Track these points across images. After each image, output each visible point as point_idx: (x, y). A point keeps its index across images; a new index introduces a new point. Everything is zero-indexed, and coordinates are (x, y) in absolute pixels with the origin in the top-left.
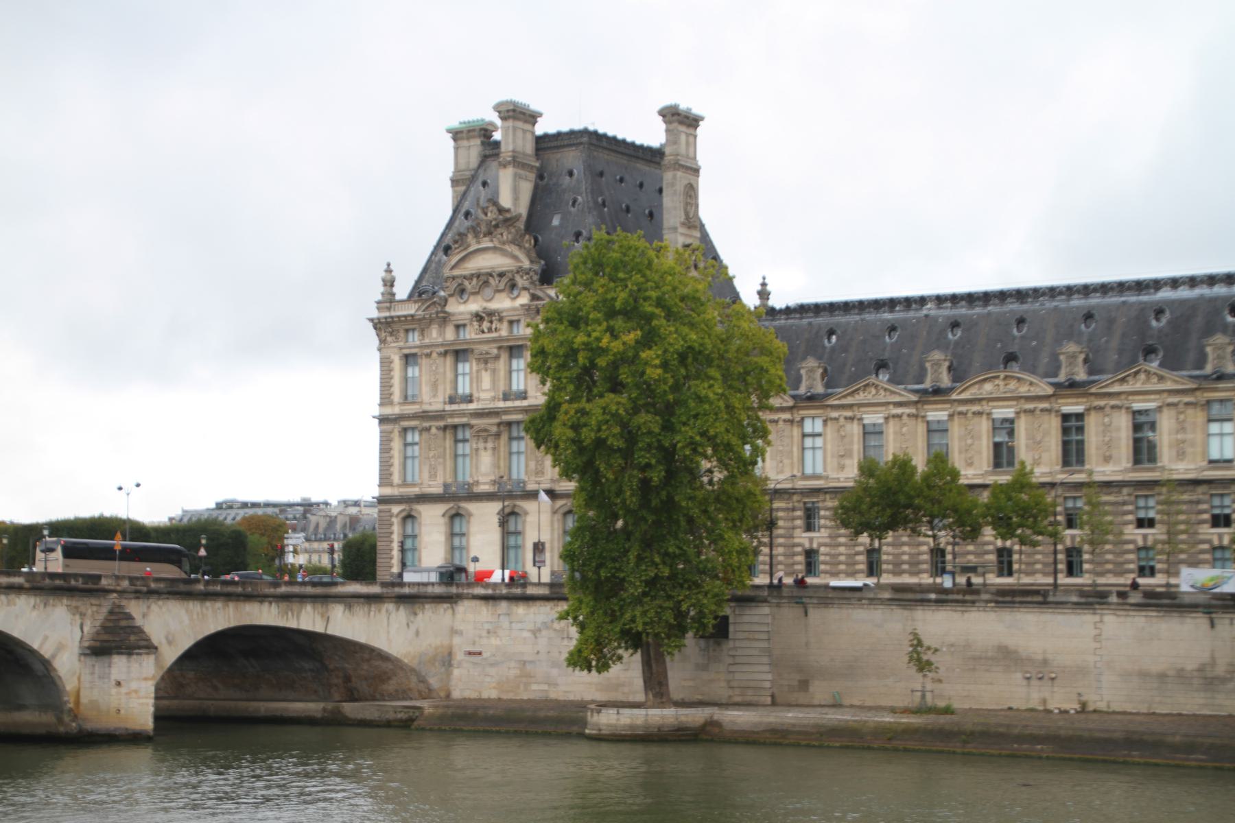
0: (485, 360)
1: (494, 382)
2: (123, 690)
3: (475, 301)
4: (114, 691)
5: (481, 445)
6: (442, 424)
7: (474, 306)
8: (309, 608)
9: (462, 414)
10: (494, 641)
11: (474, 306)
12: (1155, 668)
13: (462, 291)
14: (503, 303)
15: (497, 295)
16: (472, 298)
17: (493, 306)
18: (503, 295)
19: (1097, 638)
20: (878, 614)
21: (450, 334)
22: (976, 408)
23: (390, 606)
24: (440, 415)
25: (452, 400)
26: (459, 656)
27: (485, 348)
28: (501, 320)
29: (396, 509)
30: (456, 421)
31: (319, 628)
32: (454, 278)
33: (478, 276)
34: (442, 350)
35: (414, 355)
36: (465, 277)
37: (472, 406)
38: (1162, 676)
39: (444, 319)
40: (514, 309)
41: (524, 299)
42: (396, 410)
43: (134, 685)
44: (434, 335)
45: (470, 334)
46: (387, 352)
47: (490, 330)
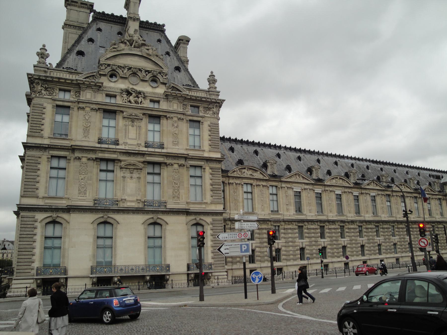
0: (133, 119)
3: (122, 83)
5: (128, 175)
6: (94, 156)
7: (122, 85)
11: (122, 85)
15: (141, 83)
16: (120, 80)
18: (146, 84)
22: (331, 189)
24: (93, 150)
28: (145, 97)
29: (40, 216)
32: (109, 65)
33: (130, 68)
34: (96, 107)
36: (120, 67)
39: (99, 87)
40: (154, 93)
41: (161, 90)
42: (46, 142)
44: (87, 95)
45: (119, 101)
47: (136, 102)
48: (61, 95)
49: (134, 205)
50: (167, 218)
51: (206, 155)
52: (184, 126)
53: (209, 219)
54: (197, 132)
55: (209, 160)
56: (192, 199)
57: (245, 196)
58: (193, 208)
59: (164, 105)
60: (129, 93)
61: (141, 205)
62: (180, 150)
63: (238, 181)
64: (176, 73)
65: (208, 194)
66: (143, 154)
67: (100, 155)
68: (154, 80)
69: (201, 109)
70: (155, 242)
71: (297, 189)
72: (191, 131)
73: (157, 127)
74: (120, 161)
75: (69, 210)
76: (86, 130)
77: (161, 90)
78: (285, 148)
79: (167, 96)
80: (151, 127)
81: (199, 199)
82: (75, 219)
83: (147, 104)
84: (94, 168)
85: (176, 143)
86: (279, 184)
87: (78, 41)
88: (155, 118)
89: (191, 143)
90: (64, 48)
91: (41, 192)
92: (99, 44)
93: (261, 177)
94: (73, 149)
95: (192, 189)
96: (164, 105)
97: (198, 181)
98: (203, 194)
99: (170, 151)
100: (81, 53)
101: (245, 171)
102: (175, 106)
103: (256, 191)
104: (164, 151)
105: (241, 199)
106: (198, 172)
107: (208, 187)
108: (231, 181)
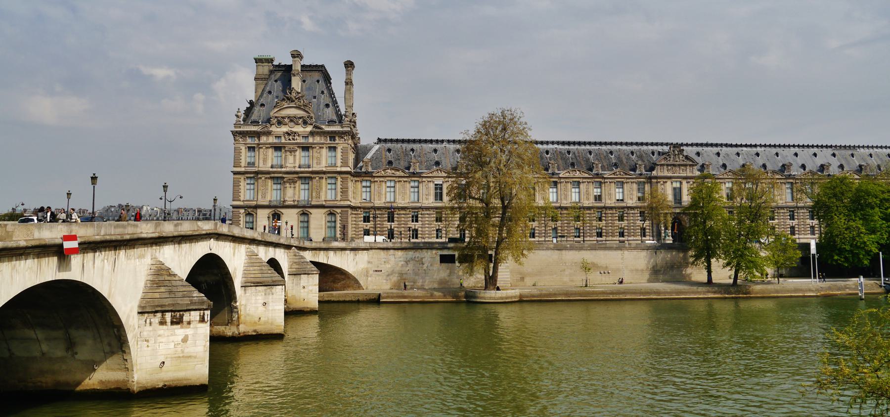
1: (295, 160)
2: (306, 290)
4: (302, 291)
7: (284, 129)
8: (322, 252)
9: (280, 172)
10: (388, 266)
11: (284, 129)
12: (640, 268)
13: (280, 123)
14: (299, 129)
17: (294, 130)
19: (622, 259)
20: (549, 252)
21: (272, 140)
23: (348, 252)
24: (268, 173)
25: (272, 167)
26: (371, 272)
27: (292, 146)
29: (242, 211)
30: (276, 175)
31: (325, 262)
35: (254, 148)
37: (283, 170)
38: (642, 270)
41: (309, 128)
42: (243, 169)
43: (310, 288)
44: (264, 139)
45: (283, 141)
46: (237, 145)
48: (249, 140)
49: (292, 203)
50: (311, 210)
51: (339, 169)
52: (324, 151)
53: (339, 210)
54: (333, 154)
55: (340, 173)
56: (329, 198)
57: (388, 189)
58: (328, 204)
59: (311, 140)
60: (289, 134)
61: (296, 203)
62: (322, 167)
63: (382, 179)
64: (326, 109)
65: (339, 194)
66: (297, 173)
67: (272, 175)
68: (305, 123)
69: (337, 138)
70: (306, 225)
71: (439, 181)
72: (330, 154)
73: (307, 153)
74: (284, 178)
75: (257, 207)
76: (265, 160)
77: (309, 128)
78: (449, 141)
79: (312, 133)
80: (303, 154)
81: (333, 198)
82: (259, 211)
83: (300, 140)
84: (270, 182)
85: (319, 163)
86: (420, 180)
87: (261, 95)
88: (306, 148)
89: (329, 162)
90: (256, 96)
91: (242, 198)
92: (275, 94)
93: (402, 174)
94: (257, 173)
95: (329, 192)
96: (311, 140)
97: (333, 187)
98: (336, 195)
99: (314, 169)
100: (263, 105)
101: (389, 171)
102: (318, 139)
103: (398, 185)
104: (310, 170)
105: (384, 193)
106: (333, 181)
107: (339, 190)
108: (376, 179)
